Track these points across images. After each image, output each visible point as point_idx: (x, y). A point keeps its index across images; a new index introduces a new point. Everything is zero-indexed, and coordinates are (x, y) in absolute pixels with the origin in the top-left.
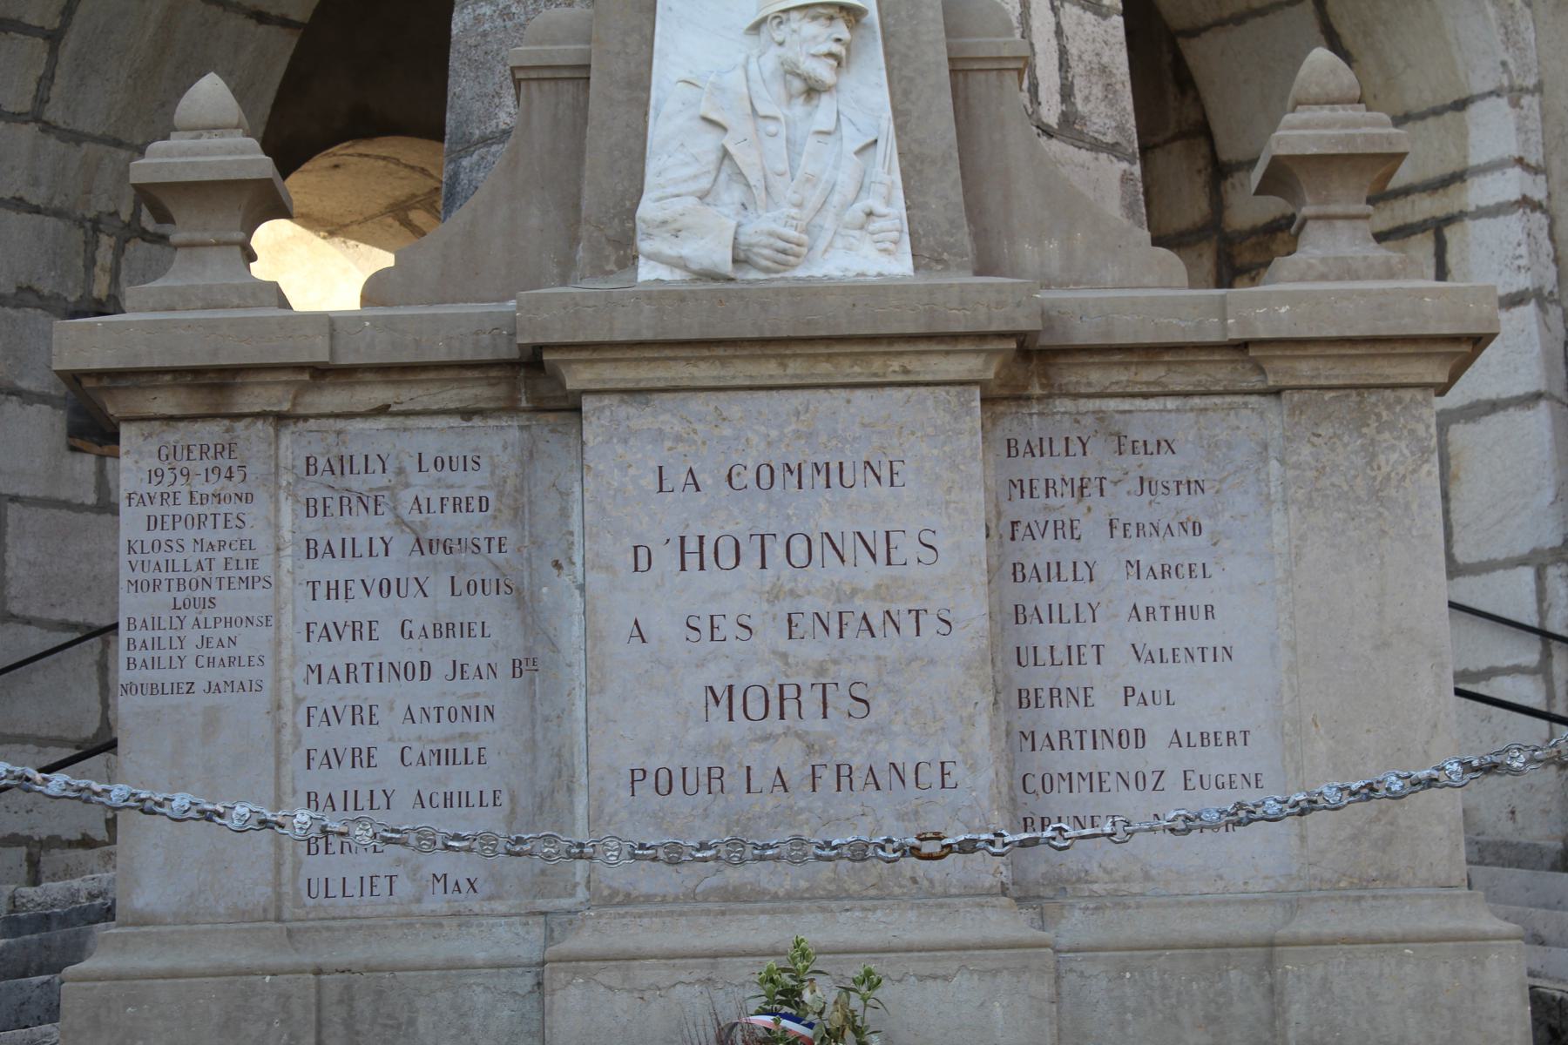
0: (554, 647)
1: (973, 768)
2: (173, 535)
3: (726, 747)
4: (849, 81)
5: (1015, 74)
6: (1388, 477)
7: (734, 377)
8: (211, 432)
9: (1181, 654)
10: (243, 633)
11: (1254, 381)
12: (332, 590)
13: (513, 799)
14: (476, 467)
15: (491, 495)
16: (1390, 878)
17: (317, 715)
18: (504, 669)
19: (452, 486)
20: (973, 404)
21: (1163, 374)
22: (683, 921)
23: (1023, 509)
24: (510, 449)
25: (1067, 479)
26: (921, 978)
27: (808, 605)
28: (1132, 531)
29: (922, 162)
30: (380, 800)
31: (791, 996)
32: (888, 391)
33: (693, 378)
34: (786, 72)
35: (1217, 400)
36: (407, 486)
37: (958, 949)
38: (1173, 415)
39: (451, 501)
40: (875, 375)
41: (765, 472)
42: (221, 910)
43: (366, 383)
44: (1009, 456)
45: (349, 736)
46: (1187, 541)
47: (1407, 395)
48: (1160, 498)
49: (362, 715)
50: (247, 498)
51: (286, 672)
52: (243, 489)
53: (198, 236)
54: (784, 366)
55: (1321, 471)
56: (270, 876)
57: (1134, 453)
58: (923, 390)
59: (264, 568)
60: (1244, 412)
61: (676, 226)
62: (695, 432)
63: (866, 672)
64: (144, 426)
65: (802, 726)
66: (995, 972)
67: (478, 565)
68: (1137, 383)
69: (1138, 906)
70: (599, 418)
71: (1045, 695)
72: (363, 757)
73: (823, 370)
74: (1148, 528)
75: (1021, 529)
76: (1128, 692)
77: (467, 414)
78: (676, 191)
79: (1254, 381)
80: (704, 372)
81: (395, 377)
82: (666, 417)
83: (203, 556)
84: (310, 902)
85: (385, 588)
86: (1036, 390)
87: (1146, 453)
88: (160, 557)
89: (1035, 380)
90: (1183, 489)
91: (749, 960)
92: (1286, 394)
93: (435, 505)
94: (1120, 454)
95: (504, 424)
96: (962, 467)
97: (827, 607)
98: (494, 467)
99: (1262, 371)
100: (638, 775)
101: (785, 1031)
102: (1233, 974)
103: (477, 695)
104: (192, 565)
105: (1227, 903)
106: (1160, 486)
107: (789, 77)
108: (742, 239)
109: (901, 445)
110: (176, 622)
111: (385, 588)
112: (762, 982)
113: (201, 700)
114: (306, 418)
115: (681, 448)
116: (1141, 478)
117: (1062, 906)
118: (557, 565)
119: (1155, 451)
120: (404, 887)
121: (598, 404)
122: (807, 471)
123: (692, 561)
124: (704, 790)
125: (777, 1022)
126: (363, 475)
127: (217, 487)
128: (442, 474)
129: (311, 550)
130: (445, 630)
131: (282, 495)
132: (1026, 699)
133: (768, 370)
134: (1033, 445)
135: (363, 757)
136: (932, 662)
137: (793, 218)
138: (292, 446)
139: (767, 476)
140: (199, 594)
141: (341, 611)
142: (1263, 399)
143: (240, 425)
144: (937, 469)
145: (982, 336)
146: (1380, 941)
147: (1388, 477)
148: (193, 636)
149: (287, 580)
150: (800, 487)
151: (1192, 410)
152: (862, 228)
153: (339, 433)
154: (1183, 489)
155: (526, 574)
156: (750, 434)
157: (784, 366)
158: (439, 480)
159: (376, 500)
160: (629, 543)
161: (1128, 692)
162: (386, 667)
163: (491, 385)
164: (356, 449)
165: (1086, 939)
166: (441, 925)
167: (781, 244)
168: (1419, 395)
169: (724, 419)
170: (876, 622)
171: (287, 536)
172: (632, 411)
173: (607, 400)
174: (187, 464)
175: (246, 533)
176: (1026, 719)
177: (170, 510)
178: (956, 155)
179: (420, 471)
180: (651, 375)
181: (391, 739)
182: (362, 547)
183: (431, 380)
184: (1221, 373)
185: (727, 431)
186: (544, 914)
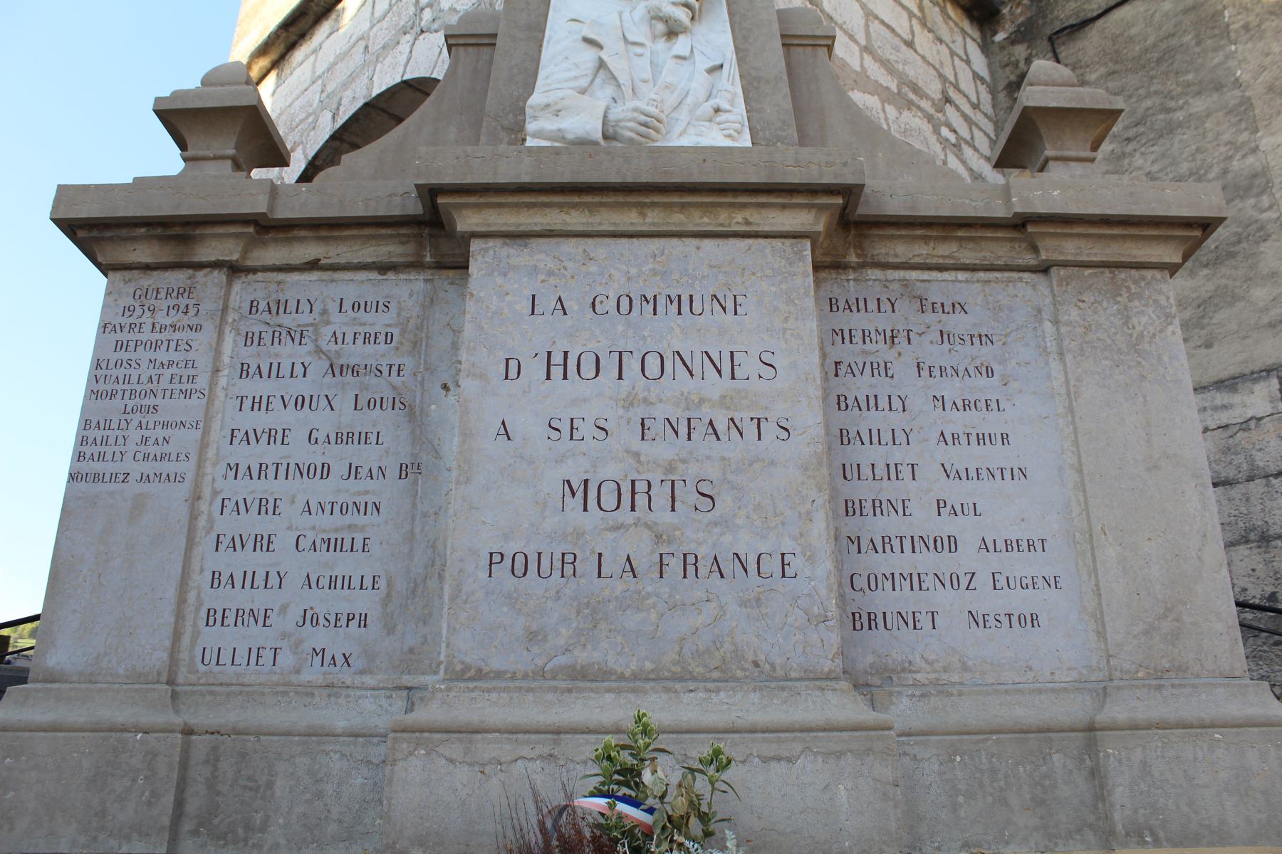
0: (437, 455)
1: (811, 559)
2: (133, 356)
3: (579, 534)
4: (700, 30)
5: (825, 49)
6: (1141, 335)
7: (600, 224)
8: (177, 278)
9: (984, 473)
10: (177, 435)
11: (1028, 259)
12: (256, 404)
13: (390, 584)
14: (386, 309)
15: (396, 332)
16: (1181, 669)
17: (230, 505)
18: (392, 472)
19: (364, 324)
20: (805, 253)
21: (955, 250)
22: (530, 697)
23: (846, 352)
24: (415, 296)
25: (880, 330)
26: (765, 760)
27: (660, 412)
28: (936, 372)
29: (759, 82)
30: (274, 580)
31: (630, 775)
32: (732, 241)
33: (566, 224)
34: (652, 18)
35: (997, 274)
36: (328, 323)
37: (802, 731)
38: (964, 284)
39: (363, 335)
40: (722, 225)
41: (624, 302)
42: (121, 672)
43: (301, 240)
44: (831, 310)
45: (252, 524)
46: (983, 381)
47: (1148, 274)
48: (958, 347)
49: (267, 507)
50: (197, 328)
51: (209, 469)
52: (194, 321)
53: (201, 153)
54: (644, 215)
55: (1088, 328)
56: (167, 643)
57: (934, 312)
58: (762, 241)
59: (202, 382)
60: (1019, 285)
61: (556, 108)
62: (565, 268)
63: (713, 471)
64: (127, 274)
65: (651, 517)
66: (839, 755)
67: (380, 387)
68: (934, 256)
69: (960, 694)
70: (483, 257)
71: (868, 506)
72: (264, 543)
73: (677, 220)
74: (949, 370)
75: (843, 369)
76: (940, 504)
77: (383, 268)
78: (559, 86)
79: (1028, 259)
80: (575, 219)
81: (323, 233)
82: (542, 256)
83: (153, 372)
84: (202, 668)
85: (300, 402)
86: (853, 258)
87: (944, 312)
88: (121, 372)
89: (852, 250)
90: (976, 341)
91: (592, 738)
92: (1054, 270)
93: (349, 338)
94: (923, 312)
95: (412, 277)
96: (796, 301)
97: (677, 414)
98: (400, 310)
99: (1035, 249)
100: (497, 558)
101: (620, 816)
102: (1056, 757)
103: (367, 492)
104: (144, 379)
105: (1040, 691)
106: (956, 338)
107: (654, 22)
108: (611, 117)
109: (743, 282)
110: (124, 424)
111: (300, 402)
112: (598, 759)
113: (133, 488)
114: (254, 270)
115: (552, 280)
116: (941, 331)
117: (891, 694)
118: (445, 387)
119: (951, 311)
120: (286, 659)
121: (484, 246)
122: (661, 301)
123: (557, 372)
124: (557, 574)
125: (612, 806)
126: (294, 315)
127: (175, 319)
128: (358, 315)
129: (244, 371)
130: (344, 438)
131: (227, 329)
132: (851, 509)
133: (629, 219)
134: (850, 303)
135: (264, 543)
136: (772, 463)
137: (654, 100)
138: (241, 292)
139: (624, 304)
140: (146, 402)
141: (260, 421)
142: (1033, 276)
143: (200, 274)
144: (775, 303)
145: (812, 190)
146: (1191, 726)
147: (1141, 335)
148: (135, 435)
149: (220, 394)
150: (655, 314)
151: (978, 281)
152: (710, 120)
153: (279, 283)
154: (976, 341)
155: (418, 395)
156: (612, 272)
157: (644, 215)
158: (355, 319)
159: (302, 334)
160: (502, 356)
161: (940, 504)
162: (292, 467)
163: (402, 243)
164: (291, 295)
165: (916, 724)
166: (313, 695)
167: (643, 118)
168: (1157, 274)
169: (591, 259)
170: (721, 426)
171: (226, 359)
172: (512, 251)
173: (491, 243)
174: (153, 301)
175: (191, 355)
176: (852, 525)
177: (134, 336)
178: (785, 77)
179: (340, 312)
180: (530, 221)
181: (290, 528)
182: (286, 370)
183: (354, 237)
184: (1000, 251)
185: (593, 268)
186: (409, 689)
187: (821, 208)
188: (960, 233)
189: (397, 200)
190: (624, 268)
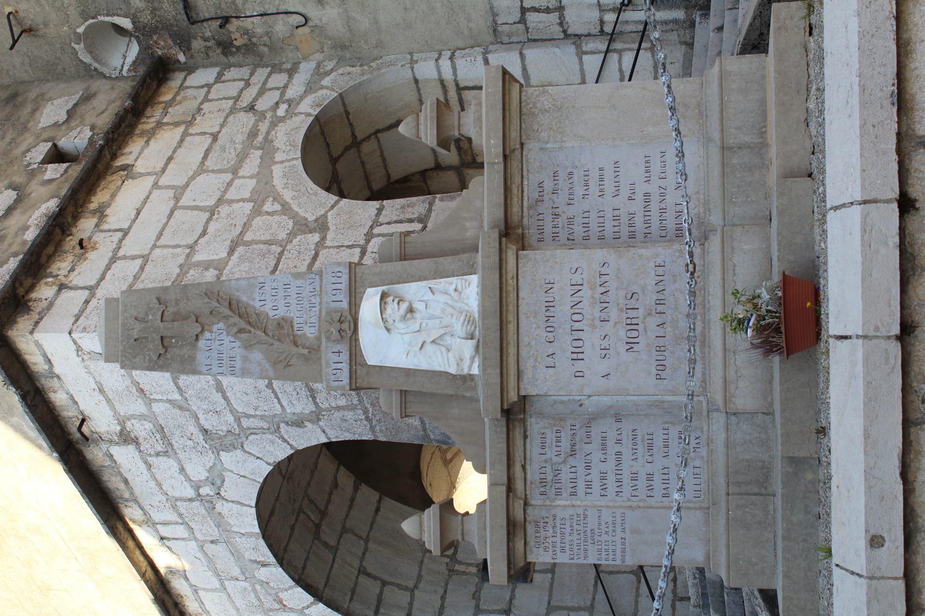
0: (612, 406)
1: (657, 255)
2: (567, 544)
3: (648, 345)
4: (408, 297)
6: (553, 105)
8: (530, 529)
9: (617, 179)
10: (604, 519)
11: (518, 153)
12: (589, 487)
13: (666, 423)
15: (555, 428)
16: (699, 105)
17: (634, 493)
18: (619, 425)
22: (712, 361)
23: (563, 236)
26: (734, 275)
27: (597, 314)
28: (571, 197)
30: (666, 471)
31: (741, 322)
32: (520, 284)
33: (514, 355)
35: (524, 166)
36: (551, 459)
37: (724, 261)
41: (549, 329)
42: (704, 529)
43: (513, 475)
45: (642, 483)
46: (575, 177)
47: (523, 98)
48: (560, 187)
49: (634, 477)
50: (555, 517)
51: (618, 504)
52: (551, 518)
53: (460, 532)
54: (510, 322)
55: (551, 129)
56: (693, 511)
58: (519, 272)
59: (580, 511)
60: (529, 156)
63: (622, 293)
64: (527, 553)
65: (641, 317)
66: (733, 248)
67: (581, 433)
69: (708, 196)
71: (631, 229)
72: (650, 477)
73: (512, 308)
74: (571, 191)
75: (570, 237)
76: (630, 199)
77: (525, 437)
79: (518, 153)
80: (512, 350)
81: (512, 462)
83: (575, 533)
84: (702, 497)
85: (588, 467)
86: (520, 231)
88: (575, 548)
90: (556, 178)
91: (727, 337)
92: (523, 141)
93: (558, 449)
97: (598, 307)
98: (545, 427)
99: (514, 150)
100: (658, 377)
101: (754, 324)
102: (734, 162)
103: (628, 435)
104: (578, 537)
105: (708, 164)
108: (464, 336)
110: (599, 543)
111: (588, 467)
112: (736, 333)
113: (628, 535)
114: (526, 495)
115: (539, 359)
117: (708, 223)
118: (581, 405)
120: (698, 463)
122: (548, 314)
123: (580, 356)
124: (664, 353)
125: (750, 327)
127: (550, 527)
129: (574, 494)
130: (604, 447)
131: (554, 504)
132: (632, 236)
133: (512, 328)
135: (650, 477)
136: (618, 269)
138: (536, 500)
139: (550, 328)
140: (589, 535)
141: (596, 484)
142: (525, 149)
143: (528, 519)
146: (722, 108)
147: (553, 105)
148: (604, 537)
149: (584, 503)
152: (460, 293)
153: (531, 483)
154: (556, 178)
155: (584, 417)
157: (510, 322)
160: (573, 379)
161: (630, 199)
162: (617, 468)
164: (537, 477)
165: (721, 215)
166: (712, 450)
167: (466, 322)
168: (524, 94)
170: (603, 290)
171: (569, 502)
172: (525, 377)
173: (522, 386)
174: (542, 539)
175: (567, 517)
176: (640, 236)
177: (558, 545)
178: (435, 259)
181: (643, 467)
182: (573, 476)
183: (513, 450)
184: (515, 164)
185: (533, 343)
186: (708, 412)
187: (506, 247)
188: (509, 184)
189: (498, 429)
190: (533, 330)
